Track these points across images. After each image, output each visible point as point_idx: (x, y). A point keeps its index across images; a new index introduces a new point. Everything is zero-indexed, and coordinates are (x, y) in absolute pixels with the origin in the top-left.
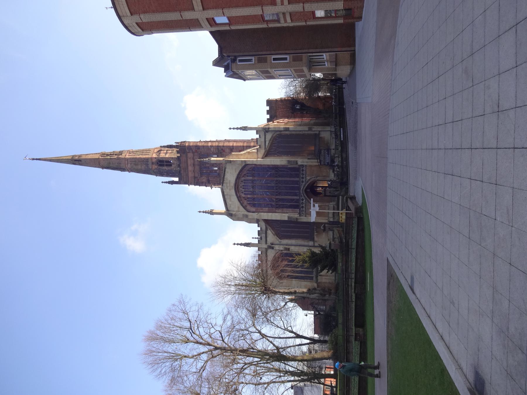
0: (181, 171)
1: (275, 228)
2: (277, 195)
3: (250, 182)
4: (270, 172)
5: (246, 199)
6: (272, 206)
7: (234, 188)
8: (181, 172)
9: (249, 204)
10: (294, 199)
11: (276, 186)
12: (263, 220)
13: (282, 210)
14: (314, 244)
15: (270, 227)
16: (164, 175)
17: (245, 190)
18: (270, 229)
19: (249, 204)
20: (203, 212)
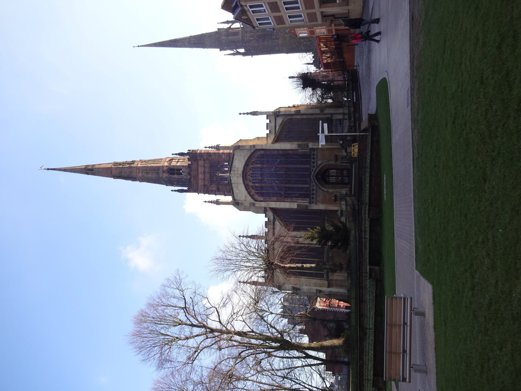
0: (191, 179)
2: (286, 183)
4: (280, 158)
5: (253, 188)
7: (241, 176)
8: (191, 180)
9: (257, 193)
10: (304, 188)
11: (286, 174)
12: (270, 208)
20: (209, 202)
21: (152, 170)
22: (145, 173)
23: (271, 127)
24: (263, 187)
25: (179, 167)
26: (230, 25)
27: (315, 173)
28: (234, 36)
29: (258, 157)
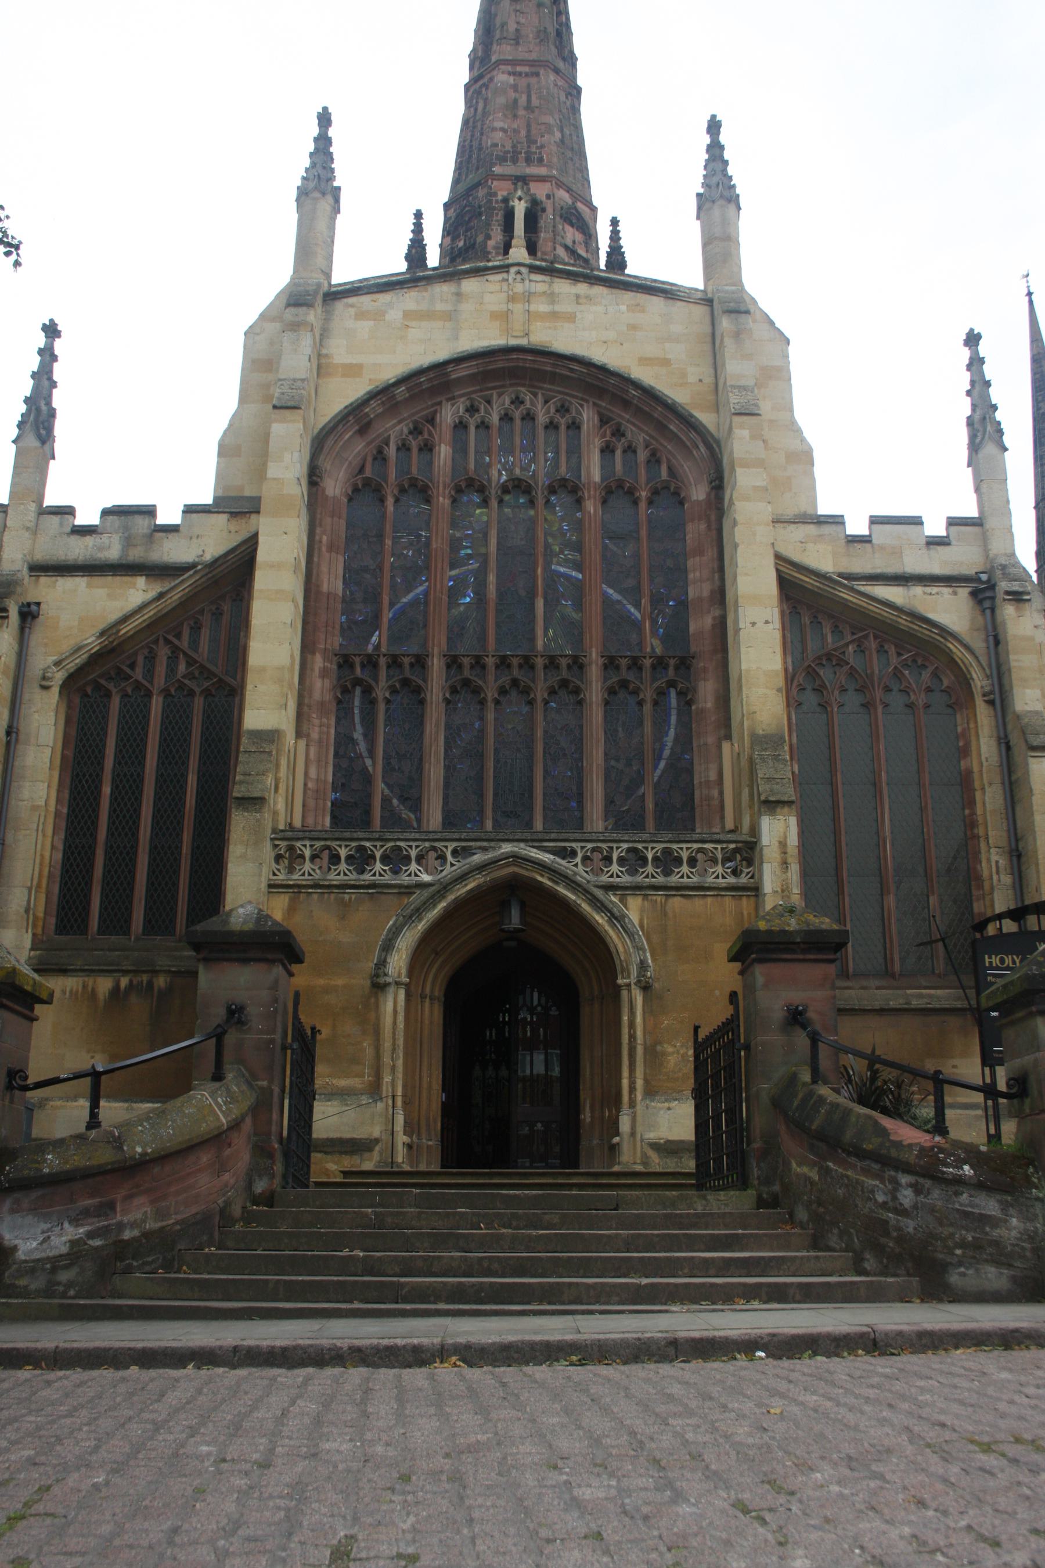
1: (167, 642)
2: (453, 662)
4: (654, 622)
5: (416, 431)
7: (513, 342)
10: (416, 804)
11: (527, 663)
12: (255, 536)
13: (322, 704)
15: (184, 604)
16: (453, 240)
17: (494, 431)
18: (161, 596)
19: (380, 456)
21: (529, 131)
22: (516, 101)
23: (897, 552)
24: (428, 501)
27: (539, 878)
29: (658, 462)
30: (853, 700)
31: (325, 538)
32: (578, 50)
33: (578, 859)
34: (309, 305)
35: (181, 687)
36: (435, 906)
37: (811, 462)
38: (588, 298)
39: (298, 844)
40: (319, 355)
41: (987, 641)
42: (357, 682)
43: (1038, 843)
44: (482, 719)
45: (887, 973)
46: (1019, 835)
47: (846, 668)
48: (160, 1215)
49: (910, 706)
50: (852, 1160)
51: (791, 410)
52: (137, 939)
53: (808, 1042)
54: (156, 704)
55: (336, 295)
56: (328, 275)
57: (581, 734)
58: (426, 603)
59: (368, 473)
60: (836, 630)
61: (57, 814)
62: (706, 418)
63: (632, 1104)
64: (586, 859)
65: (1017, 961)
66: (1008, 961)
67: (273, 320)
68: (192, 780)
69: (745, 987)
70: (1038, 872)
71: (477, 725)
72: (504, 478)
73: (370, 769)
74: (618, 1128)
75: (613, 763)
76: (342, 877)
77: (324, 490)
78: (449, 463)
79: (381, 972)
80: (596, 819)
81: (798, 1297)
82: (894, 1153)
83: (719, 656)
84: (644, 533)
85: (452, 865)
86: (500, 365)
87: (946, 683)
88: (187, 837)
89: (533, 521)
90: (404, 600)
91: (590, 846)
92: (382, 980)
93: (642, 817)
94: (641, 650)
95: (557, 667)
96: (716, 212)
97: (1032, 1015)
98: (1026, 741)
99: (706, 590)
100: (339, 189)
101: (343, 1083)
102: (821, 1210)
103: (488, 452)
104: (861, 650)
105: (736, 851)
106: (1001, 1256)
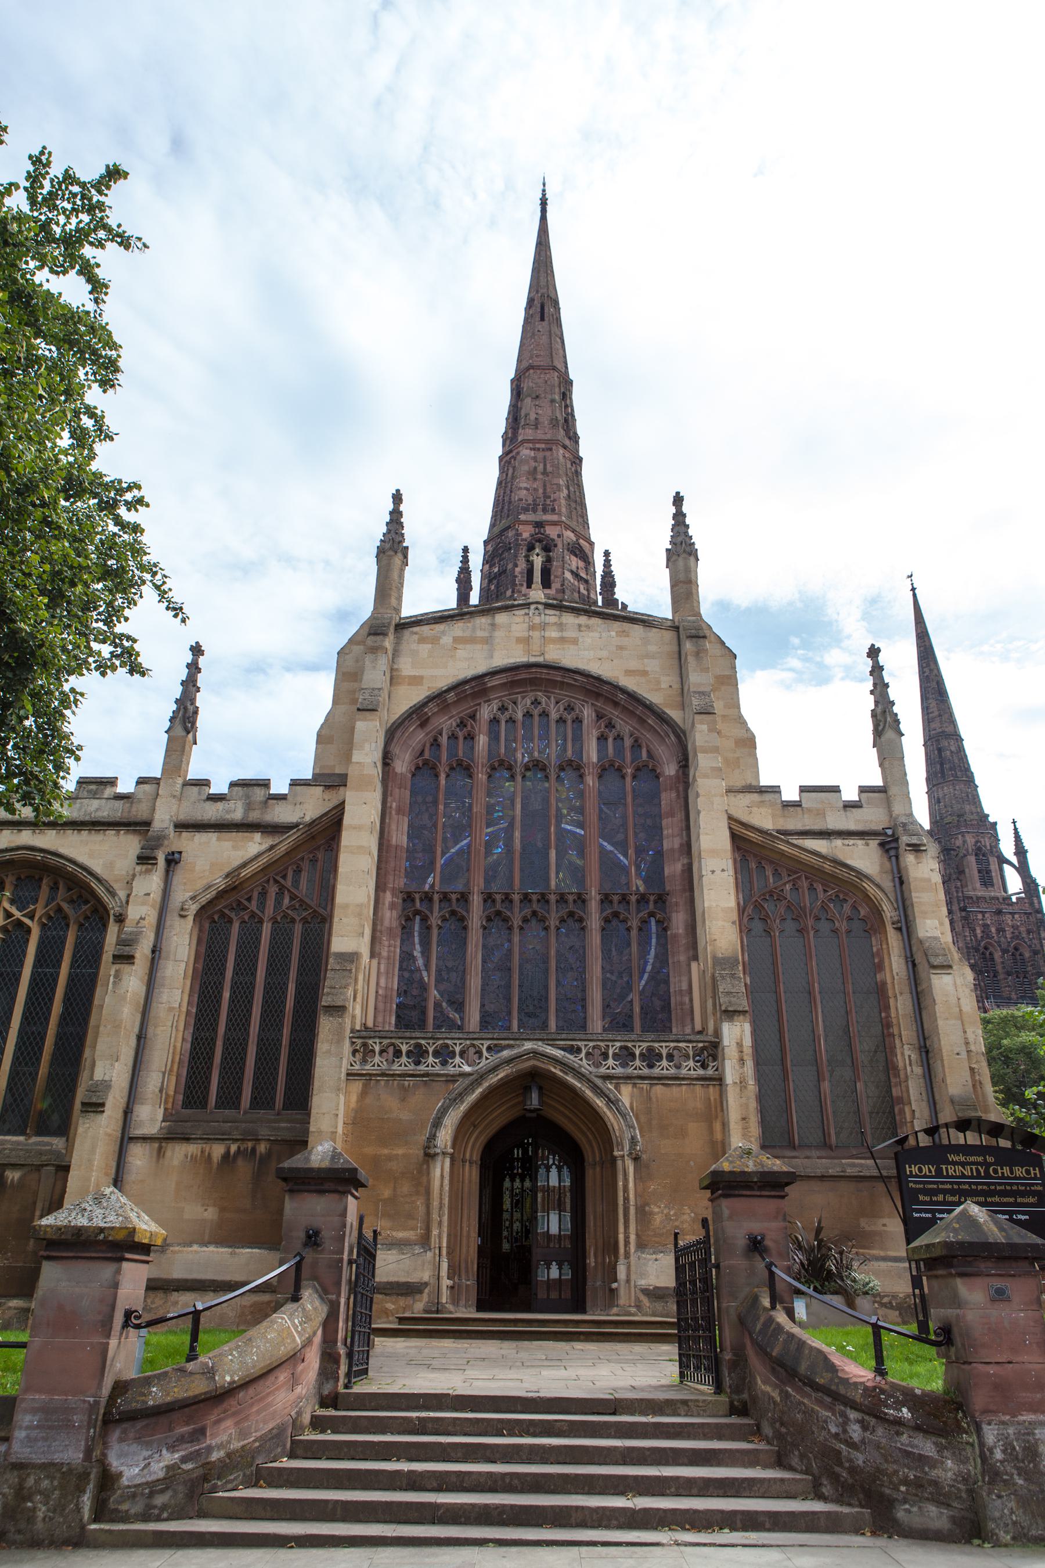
1: (276, 881)
2: (488, 898)
3: (569, 753)
4: (638, 867)
5: (462, 724)
6: (418, 871)
7: (533, 660)
9: (435, 743)
10: (459, 1006)
11: (544, 899)
12: (344, 802)
13: (390, 929)
14: (144, 1139)
15: (288, 853)
16: (490, 567)
17: (519, 725)
18: (272, 847)
19: (435, 743)
21: (545, 490)
22: (535, 468)
23: (821, 814)
24: (470, 776)
25: (556, 577)
26: (1014, 860)
27: (553, 1070)
28: (979, 872)
29: (640, 746)
30: (790, 926)
31: (394, 804)
32: (579, 432)
33: (583, 1055)
34: (385, 634)
35: (286, 915)
36: (473, 1091)
37: (754, 746)
38: (588, 627)
39: (370, 1042)
40: (392, 669)
41: (893, 881)
42: (417, 912)
43: (942, 1043)
44: (510, 941)
45: (826, 1145)
46: (926, 1034)
47: (784, 902)
48: (243, 1434)
49: (835, 931)
50: (808, 1389)
51: (739, 707)
52: (245, 1113)
53: (766, 1273)
54: (266, 929)
55: (405, 625)
56: (398, 610)
57: (584, 953)
58: (469, 853)
59: (427, 755)
60: (776, 873)
61: (188, 1013)
62: (675, 714)
63: (627, 1255)
64: (588, 1054)
65: (933, 1170)
66: (925, 1170)
67: (358, 643)
68: (291, 987)
69: (714, 1213)
70: (943, 1066)
71: (506, 946)
72: (526, 759)
73: (426, 979)
74: (616, 1273)
75: (608, 975)
76: (403, 1067)
77: (394, 769)
78: (486, 748)
79: (431, 1145)
80: (596, 1023)
81: (767, 1526)
82: (842, 1390)
83: (687, 894)
84: (629, 799)
85: (487, 1059)
86: (523, 676)
87: (862, 913)
88: (286, 1032)
89: (548, 791)
90: (453, 850)
91: (591, 1044)
92: (432, 1151)
93: (631, 1017)
94: (628, 889)
95: (566, 902)
96: (681, 563)
97: (951, 1275)
98: (928, 961)
99: (676, 843)
100: (407, 548)
101: (400, 1235)
102: (783, 1430)
103: (515, 741)
104: (795, 888)
105: (703, 1049)
106: (941, 1498)
